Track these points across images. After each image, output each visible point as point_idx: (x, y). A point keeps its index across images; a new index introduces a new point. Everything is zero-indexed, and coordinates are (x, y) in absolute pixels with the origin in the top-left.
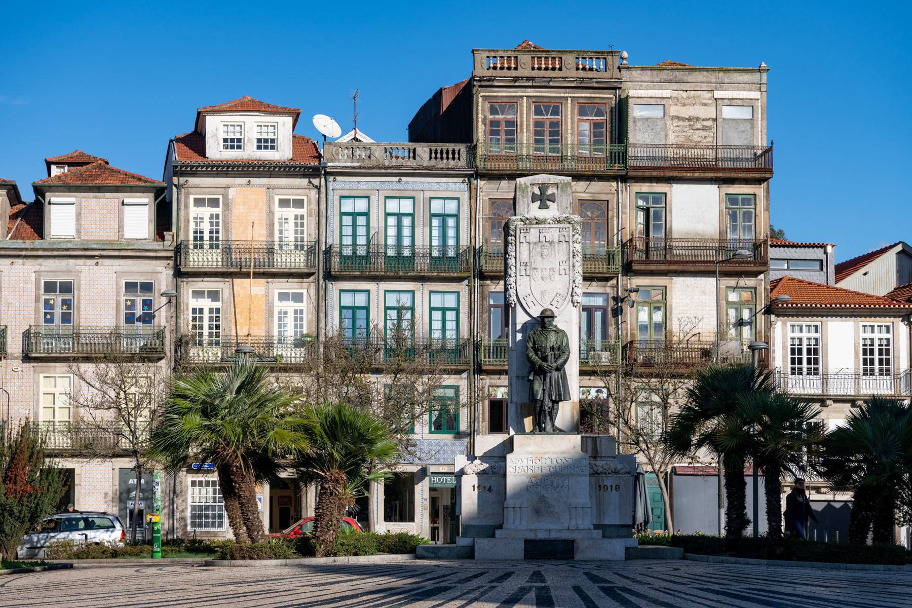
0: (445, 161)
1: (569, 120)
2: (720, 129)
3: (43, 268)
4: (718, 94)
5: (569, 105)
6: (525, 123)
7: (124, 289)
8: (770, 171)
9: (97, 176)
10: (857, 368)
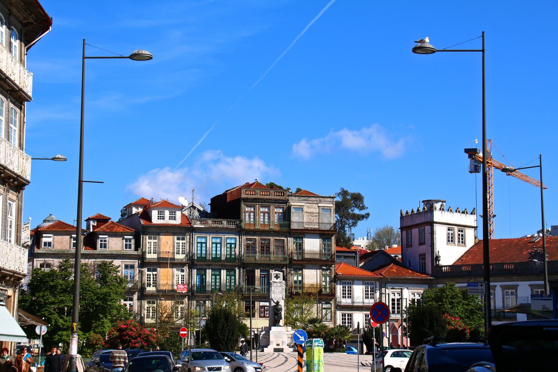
0: (232, 225)
2: (320, 216)
4: (320, 205)
7: (124, 267)
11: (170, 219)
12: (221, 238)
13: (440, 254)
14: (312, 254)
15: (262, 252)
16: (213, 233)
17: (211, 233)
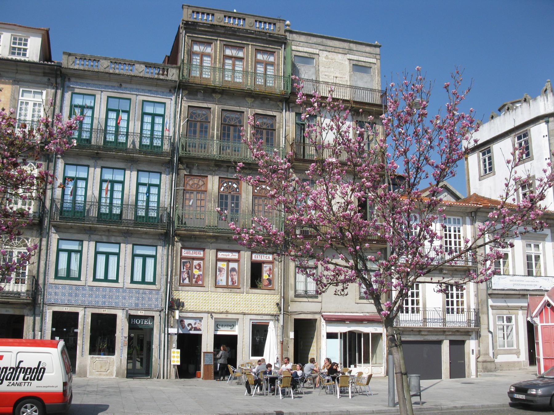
1: (250, 60)
5: (250, 50)
6: (218, 58)
12: (130, 99)
15: (224, 135)
16: (113, 87)
17: (107, 87)
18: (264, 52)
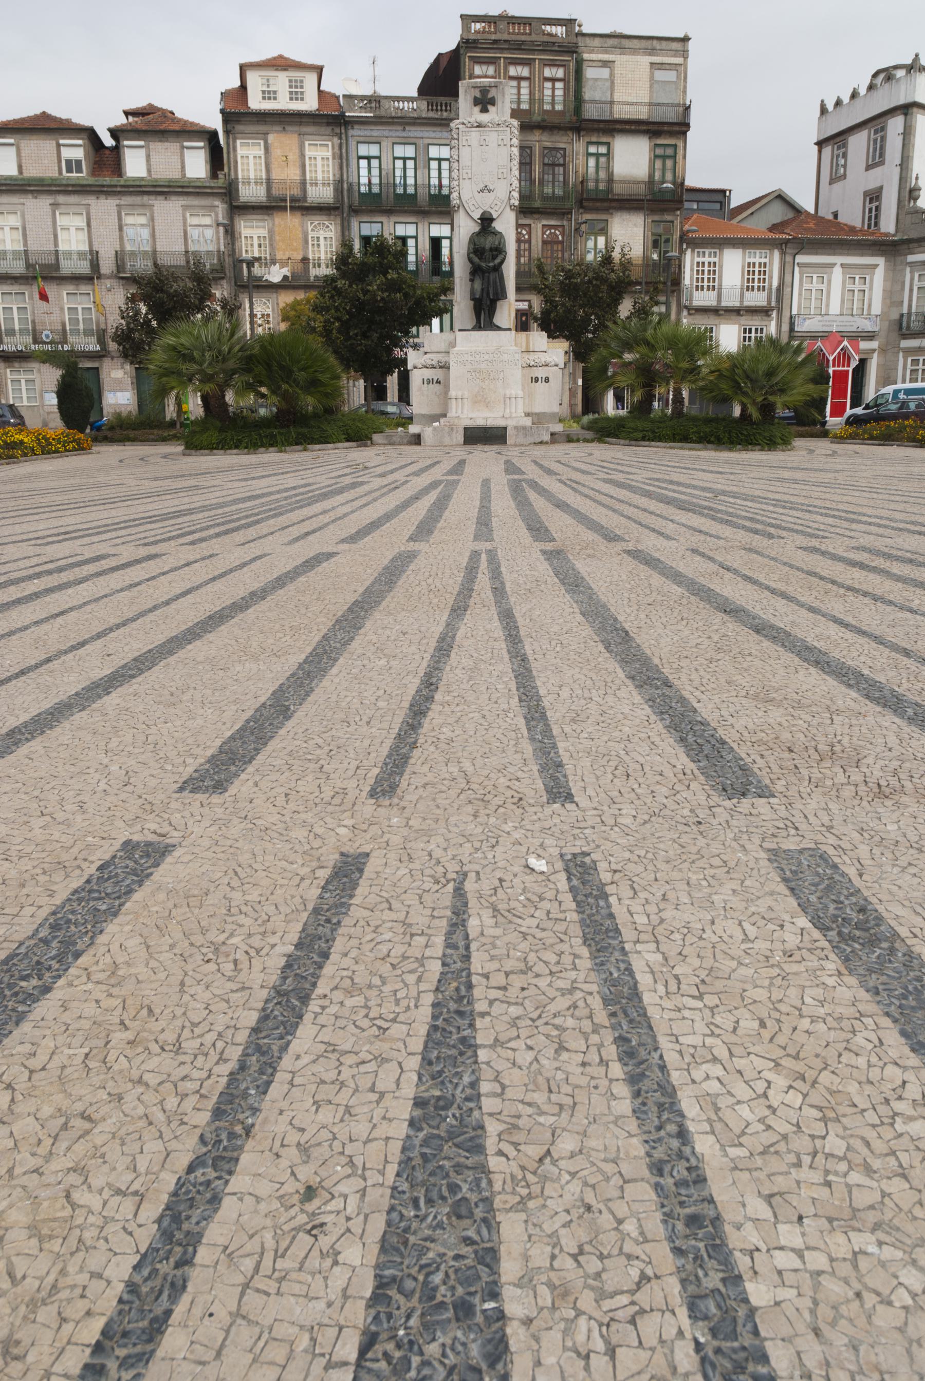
3: (122, 202)
8: (688, 126)
9: (162, 123)
10: (742, 286)
11: (291, 99)
13: (921, 183)
14: (629, 182)
18: (552, 64)
